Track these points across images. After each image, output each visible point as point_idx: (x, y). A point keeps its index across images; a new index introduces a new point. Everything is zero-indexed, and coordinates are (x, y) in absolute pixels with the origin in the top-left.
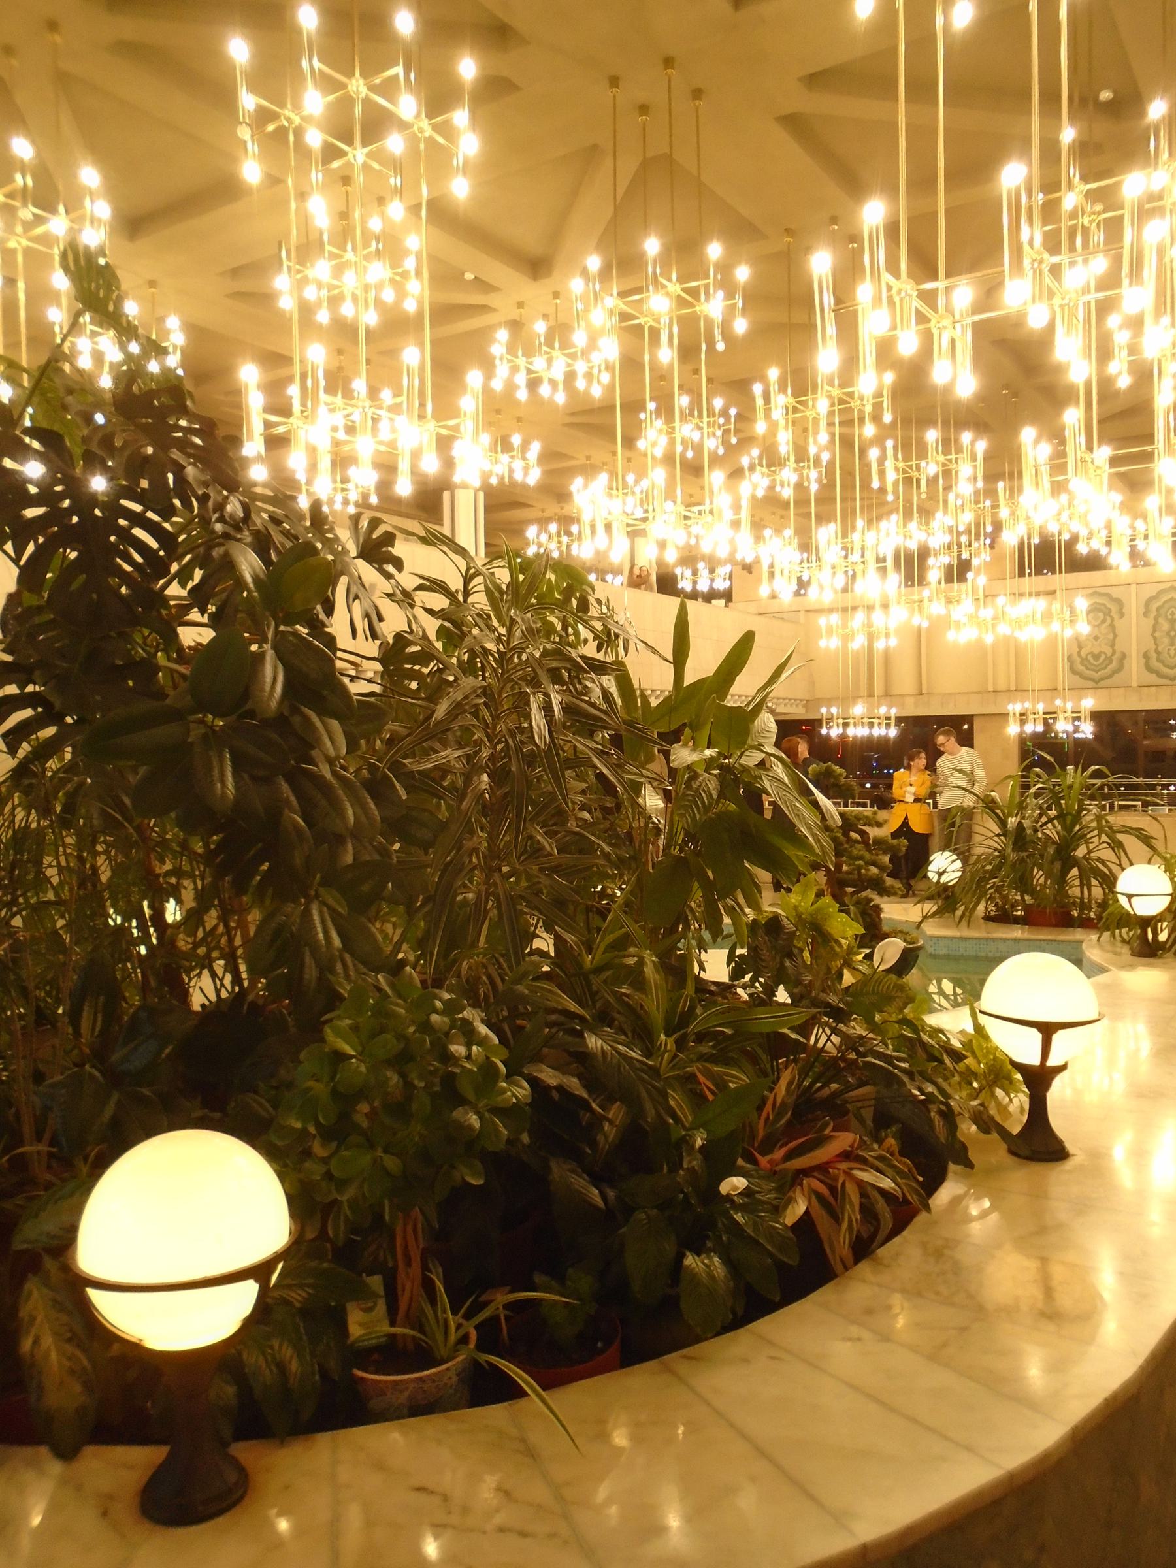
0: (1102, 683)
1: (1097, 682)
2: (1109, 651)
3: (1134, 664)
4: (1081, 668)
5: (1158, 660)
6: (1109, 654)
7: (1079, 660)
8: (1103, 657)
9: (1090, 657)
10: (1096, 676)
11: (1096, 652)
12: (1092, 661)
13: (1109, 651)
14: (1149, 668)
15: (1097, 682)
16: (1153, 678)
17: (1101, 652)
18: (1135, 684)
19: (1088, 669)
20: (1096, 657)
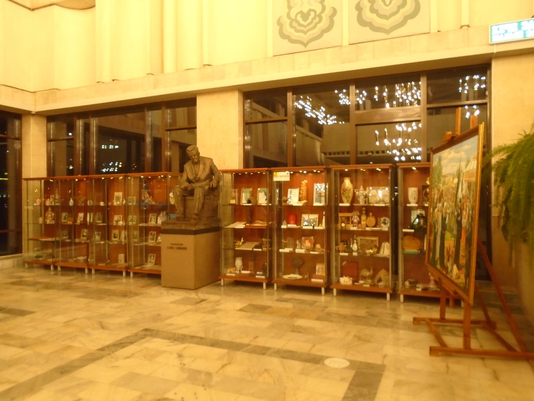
0: (311, 46)
1: (305, 45)
2: (319, 9)
3: (346, 17)
4: (288, 30)
5: (373, 10)
6: (318, 12)
7: (289, 21)
8: (312, 14)
9: (299, 18)
10: (304, 37)
11: (305, 11)
12: (302, 22)
13: (318, 8)
14: (361, 21)
15: (305, 45)
16: (367, 33)
17: (310, 10)
18: (346, 43)
19: (297, 31)
20: (305, 16)
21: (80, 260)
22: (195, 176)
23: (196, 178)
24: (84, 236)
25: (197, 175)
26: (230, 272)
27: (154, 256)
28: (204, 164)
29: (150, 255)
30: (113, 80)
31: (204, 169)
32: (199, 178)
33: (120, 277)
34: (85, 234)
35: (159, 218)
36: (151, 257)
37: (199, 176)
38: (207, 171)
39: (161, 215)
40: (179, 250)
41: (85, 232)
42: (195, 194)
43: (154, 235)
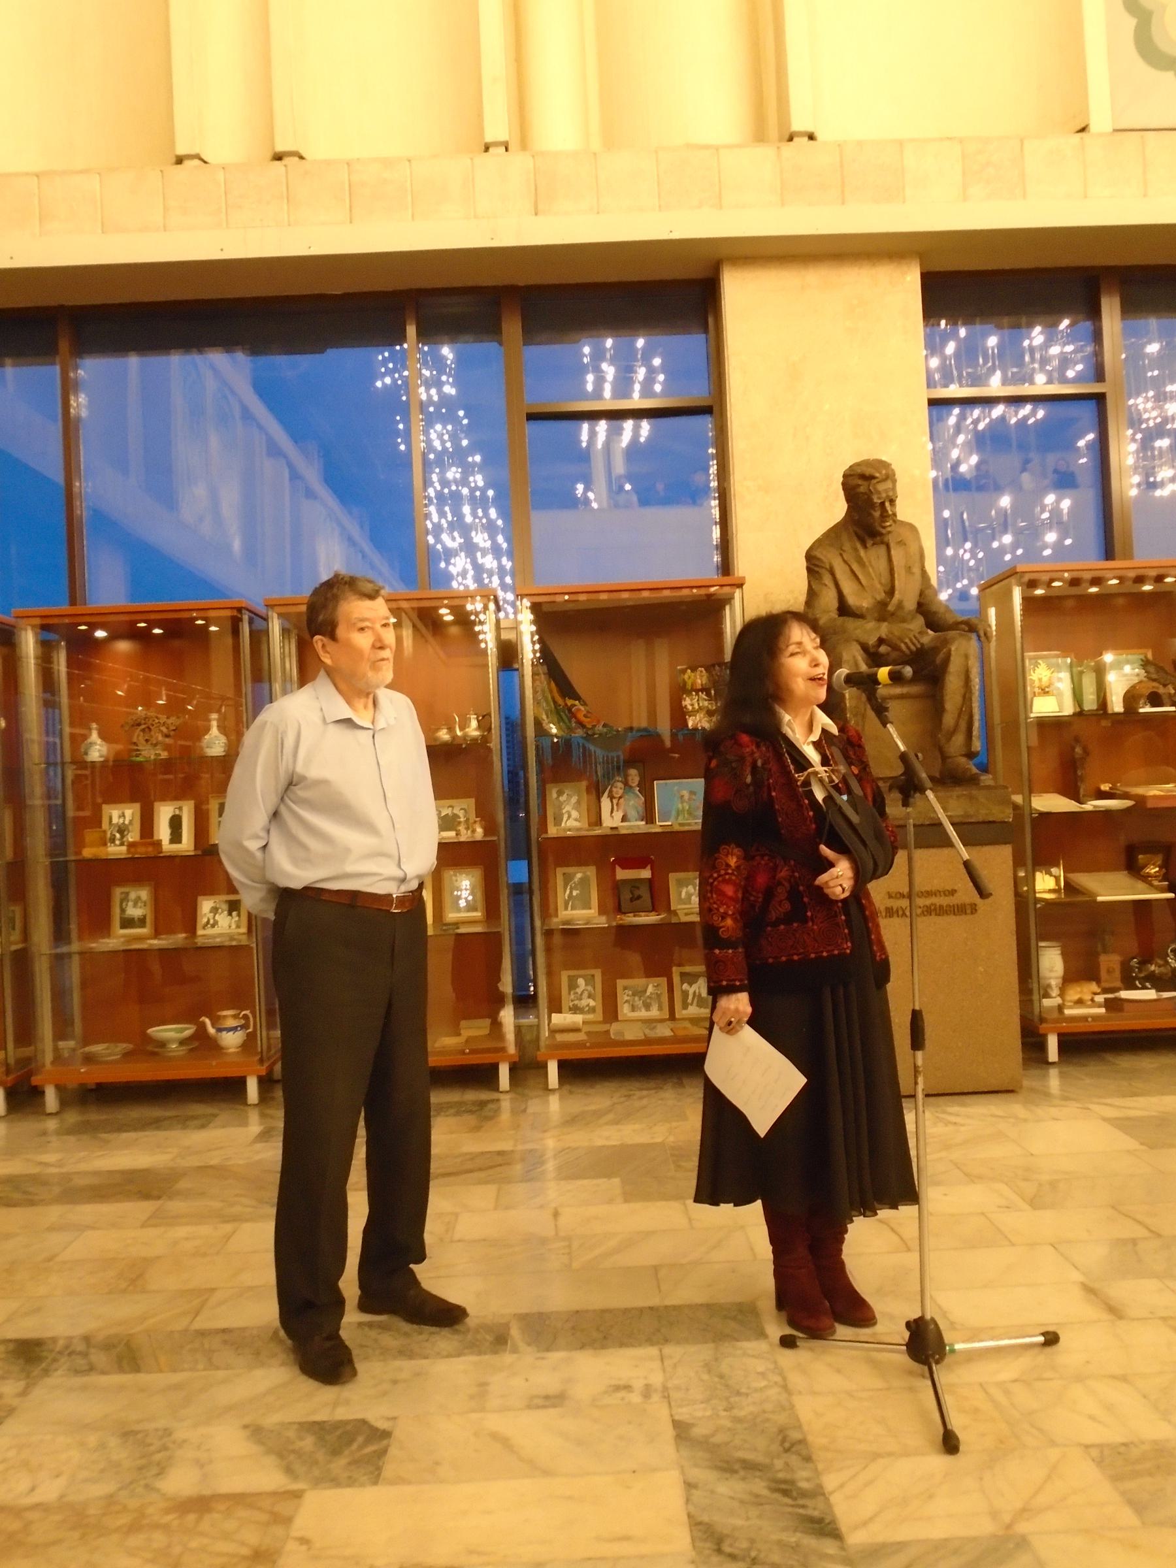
21: (163, 1044)
22: (881, 596)
23: (883, 605)
24: (127, 923)
25: (891, 592)
26: (1080, 1002)
27: (590, 980)
28: (901, 543)
29: (564, 976)
30: (278, 157)
31: (909, 569)
32: (900, 606)
33: (224, 1113)
34: (134, 912)
35: (606, 803)
36: (573, 986)
37: (897, 595)
38: (916, 570)
39: (619, 789)
40: (934, 918)
41: (136, 902)
42: (955, 666)
43: (584, 882)
